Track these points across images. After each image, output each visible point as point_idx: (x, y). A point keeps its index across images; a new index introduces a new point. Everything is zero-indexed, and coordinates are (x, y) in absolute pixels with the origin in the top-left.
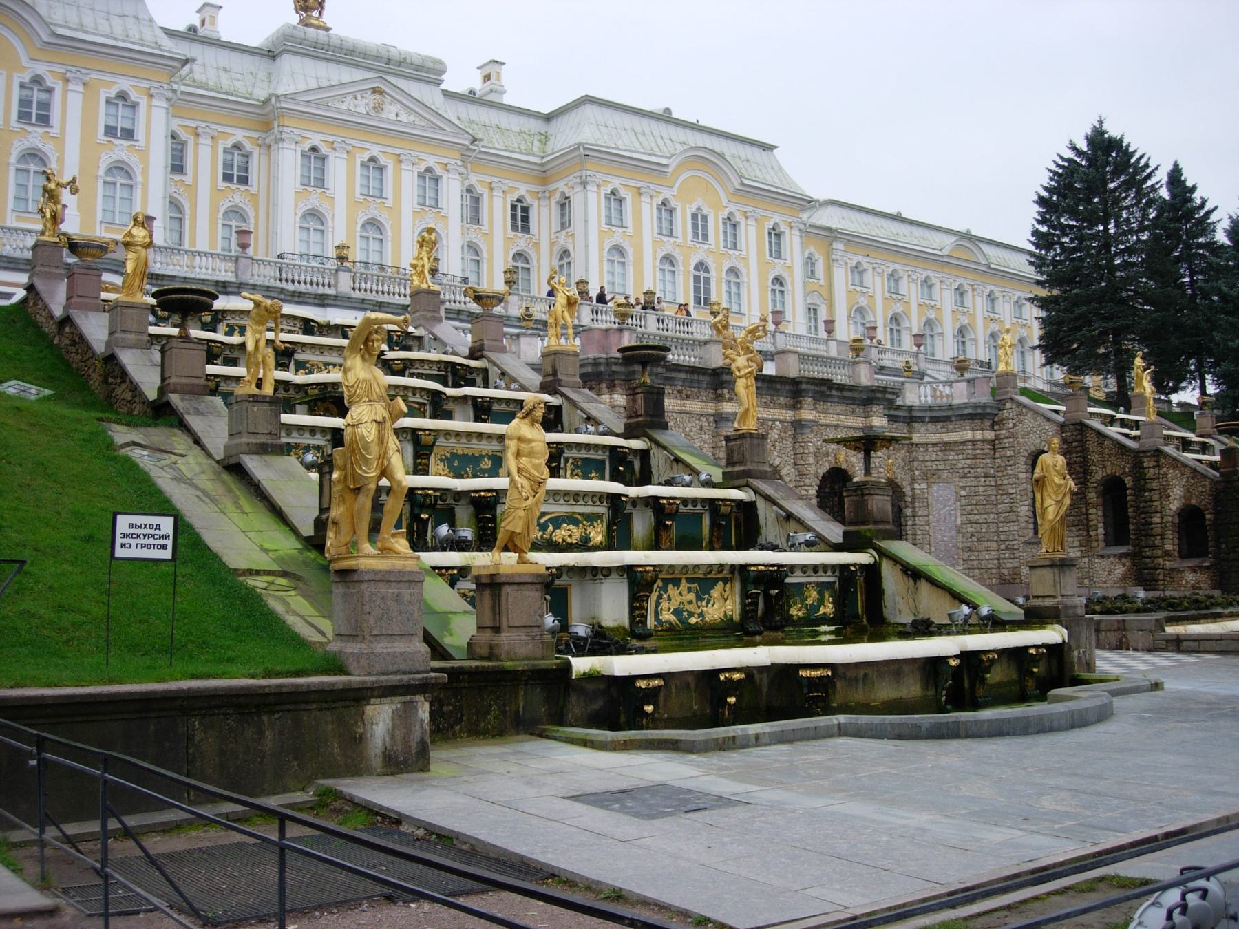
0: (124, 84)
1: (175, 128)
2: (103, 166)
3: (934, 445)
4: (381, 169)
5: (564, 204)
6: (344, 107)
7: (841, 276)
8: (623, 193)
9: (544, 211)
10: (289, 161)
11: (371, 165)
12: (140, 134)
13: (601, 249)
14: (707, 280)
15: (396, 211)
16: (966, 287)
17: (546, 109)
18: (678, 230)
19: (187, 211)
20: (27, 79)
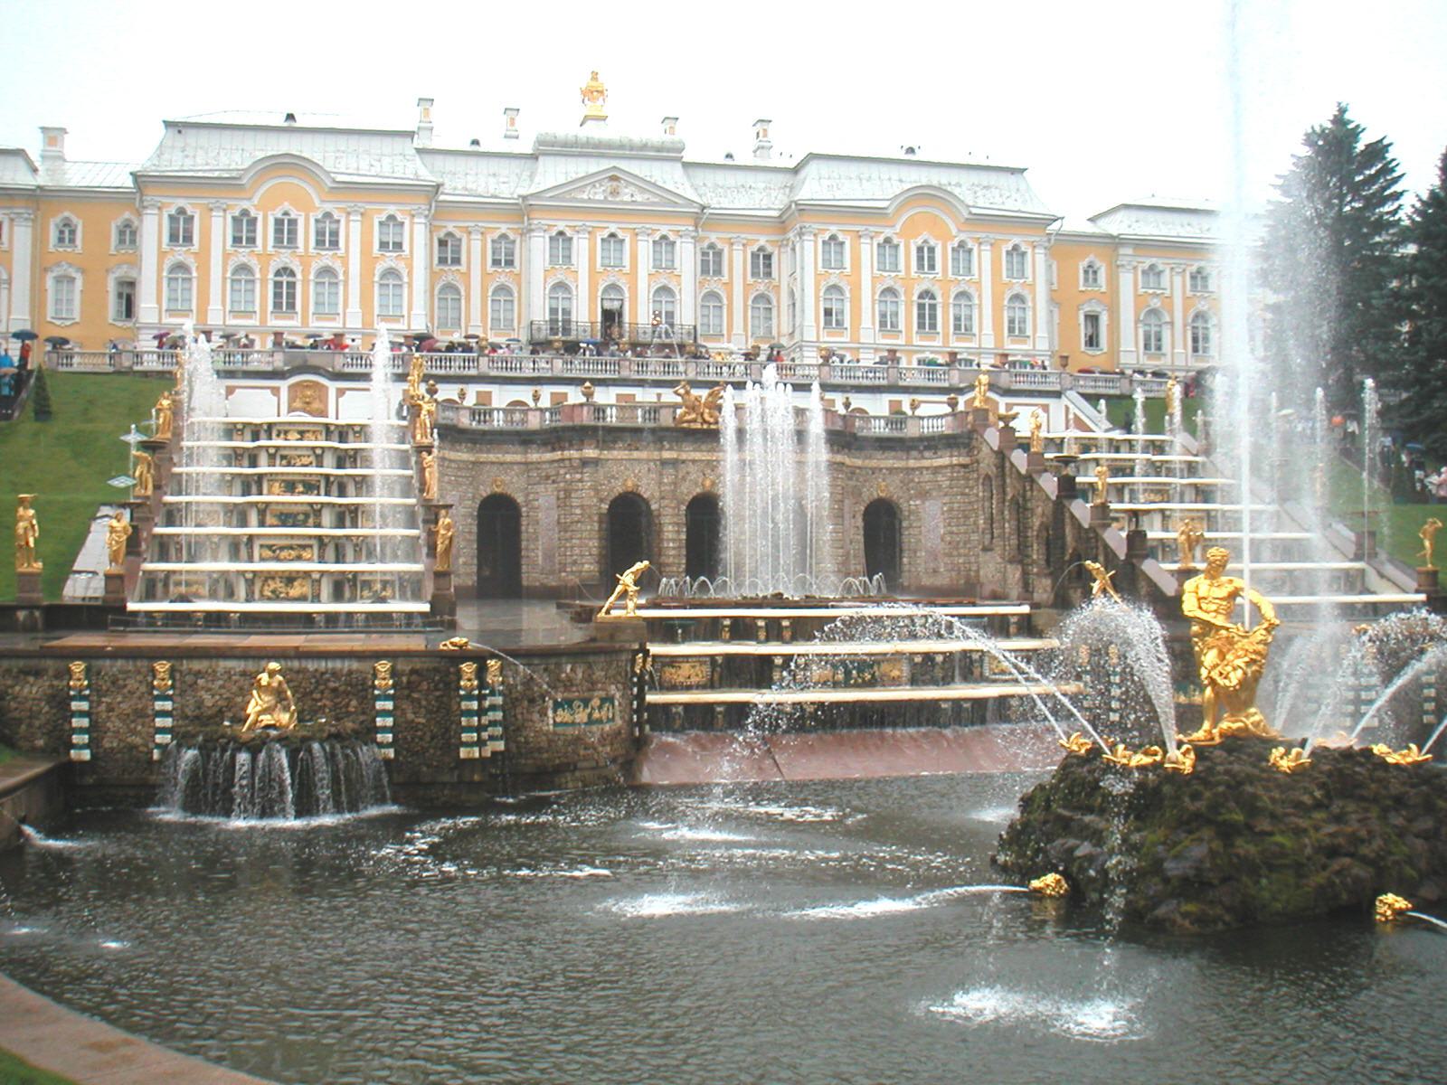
0: (392, 210)
1: (450, 227)
3: (927, 468)
4: (623, 241)
5: (793, 249)
6: (585, 196)
7: (1126, 281)
8: (841, 238)
9: (783, 257)
10: (538, 247)
11: (612, 240)
12: (406, 246)
13: (817, 290)
14: (933, 307)
15: (634, 275)
17: (792, 165)
18: (902, 266)
19: (463, 293)
20: (320, 217)
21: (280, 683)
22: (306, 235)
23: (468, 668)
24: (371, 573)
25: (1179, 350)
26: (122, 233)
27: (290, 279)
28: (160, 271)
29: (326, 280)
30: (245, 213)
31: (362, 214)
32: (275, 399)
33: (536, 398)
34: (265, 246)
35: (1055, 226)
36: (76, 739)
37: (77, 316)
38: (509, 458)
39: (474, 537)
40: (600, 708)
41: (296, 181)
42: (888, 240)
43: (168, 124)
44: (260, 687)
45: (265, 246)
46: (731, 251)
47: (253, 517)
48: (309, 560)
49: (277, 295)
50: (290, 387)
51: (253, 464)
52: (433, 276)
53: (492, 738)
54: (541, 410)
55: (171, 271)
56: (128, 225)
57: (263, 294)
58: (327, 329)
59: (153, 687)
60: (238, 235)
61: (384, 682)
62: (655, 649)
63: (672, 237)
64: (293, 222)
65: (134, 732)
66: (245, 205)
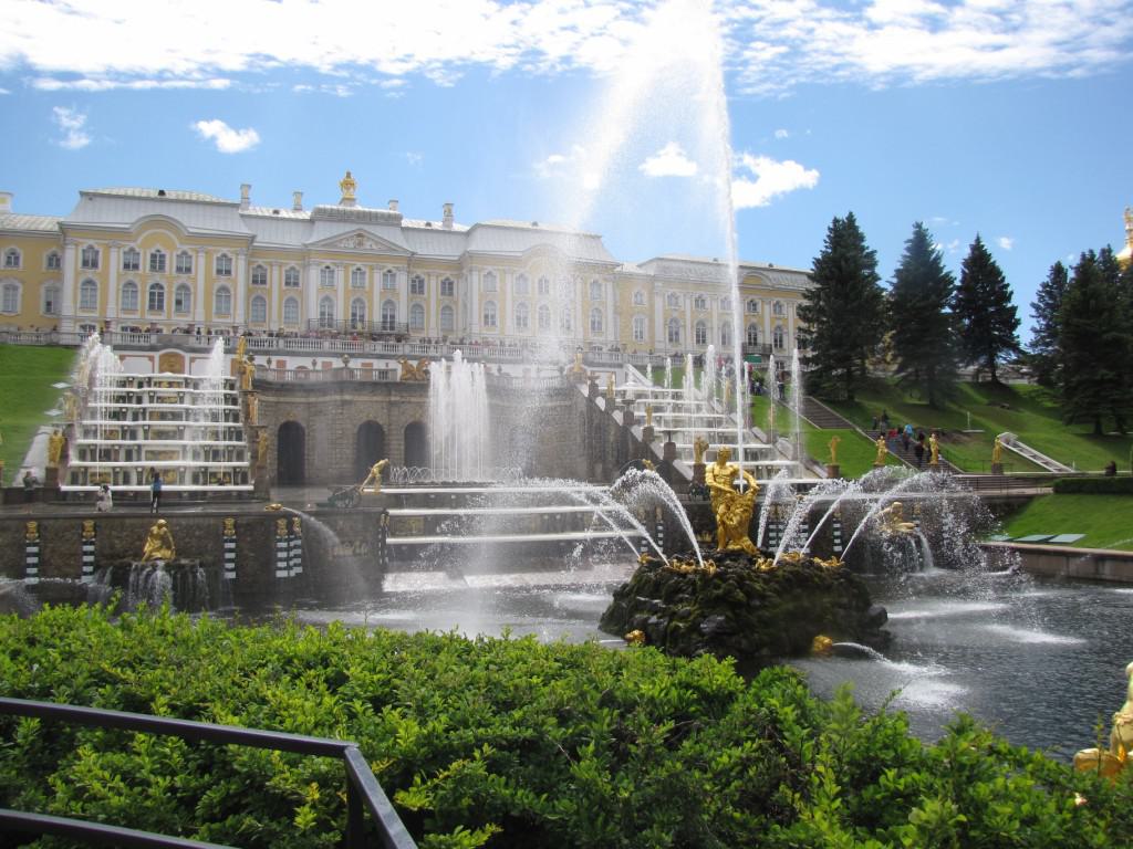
0: (224, 250)
2: (216, 287)
4: (364, 273)
5: (466, 279)
7: (659, 303)
12: (233, 273)
16: (757, 301)
20: (179, 253)
21: (165, 532)
22: (171, 263)
23: (282, 523)
24: (216, 467)
25: (689, 341)
26: (50, 259)
28: (76, 282)
30: (132, 250)
31: (206, 253)
32: (150, 363)
33: (314, 364)
34: (144, 270)
35: (618, 269)
36: (29, 571)
37: (19, 310)
38: (298, 400)
39: (276, 448)
40: (360, 546)
41: (167, 232)
42: (522, 276)
43: (83, 194)
44: (152, 535)
45: (144, 270)
46: (429, 280)
47: (141, 433)
48: (177, 459)
49: (152, 300)
50: (161, 357)
51: (139, 400)
52: (249, 292)
53: (295, 565)
54: (317, 371)
55: (84, 284)
56: (55, 255)
57: (143, 299)
58: (183, 321)
59: (83, 537)
61: (230, 531)
62: (392, 512)
63: (394, 271)
64: (163, 256)
65: (69, 565)
66: (132, 245)
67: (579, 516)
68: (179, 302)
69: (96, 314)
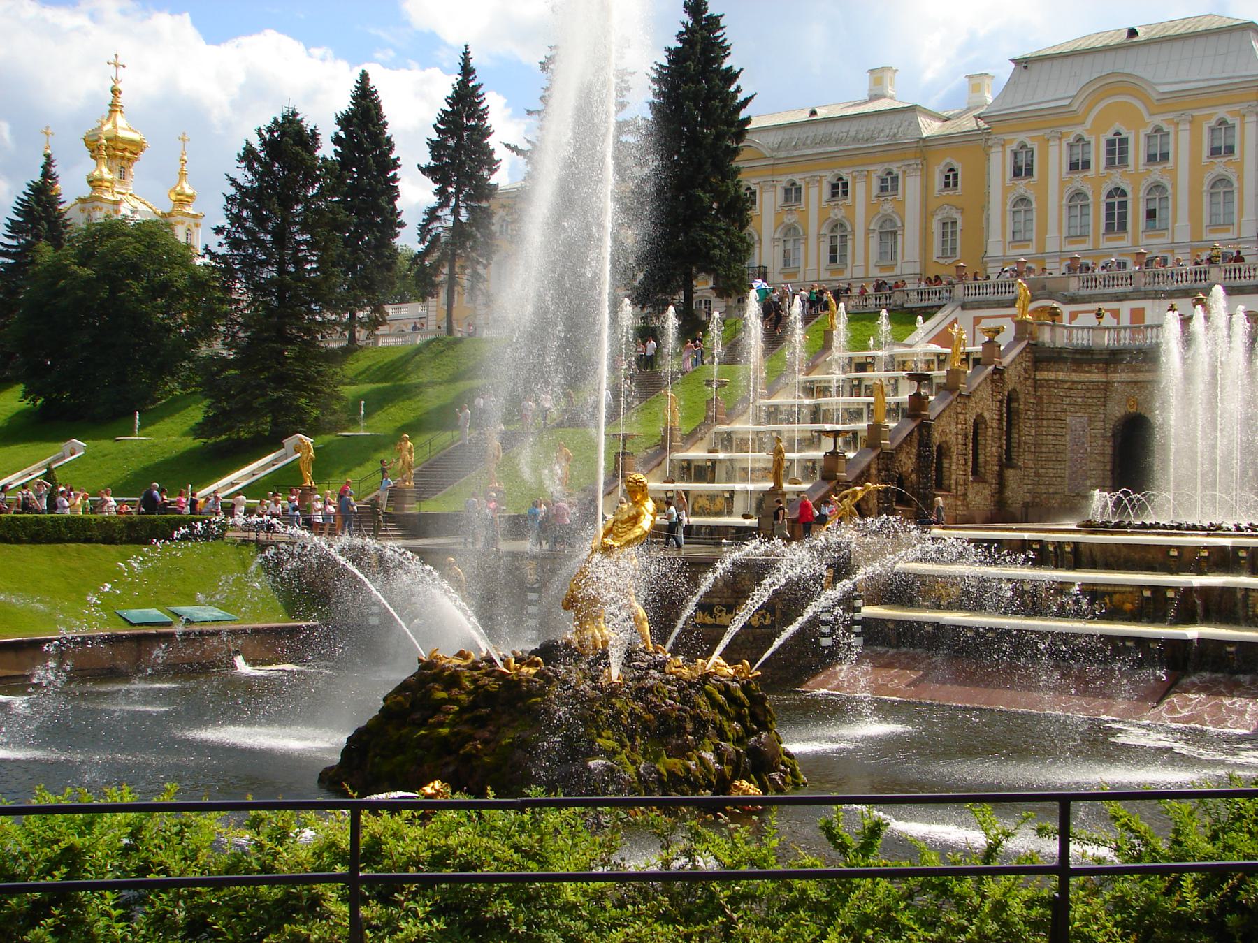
0: (1222, 112)
12: (1237, 150)
20: (1149, 130)
22: (1137, 153)
27: (1123, 199)
28: (1004, 204)
29: (1157, 195)
30: (1080, 139)
31: (1190, 122)
39: (1108, 459)
43: (1017, 62)
49: (1109, 217)
58: (1150, 245)
60: (1074, 158)
64: (1124, 141)
66: (1079, 130)
67: (1239, 595)
68: (1151, 214)
69: (1031, 250)
